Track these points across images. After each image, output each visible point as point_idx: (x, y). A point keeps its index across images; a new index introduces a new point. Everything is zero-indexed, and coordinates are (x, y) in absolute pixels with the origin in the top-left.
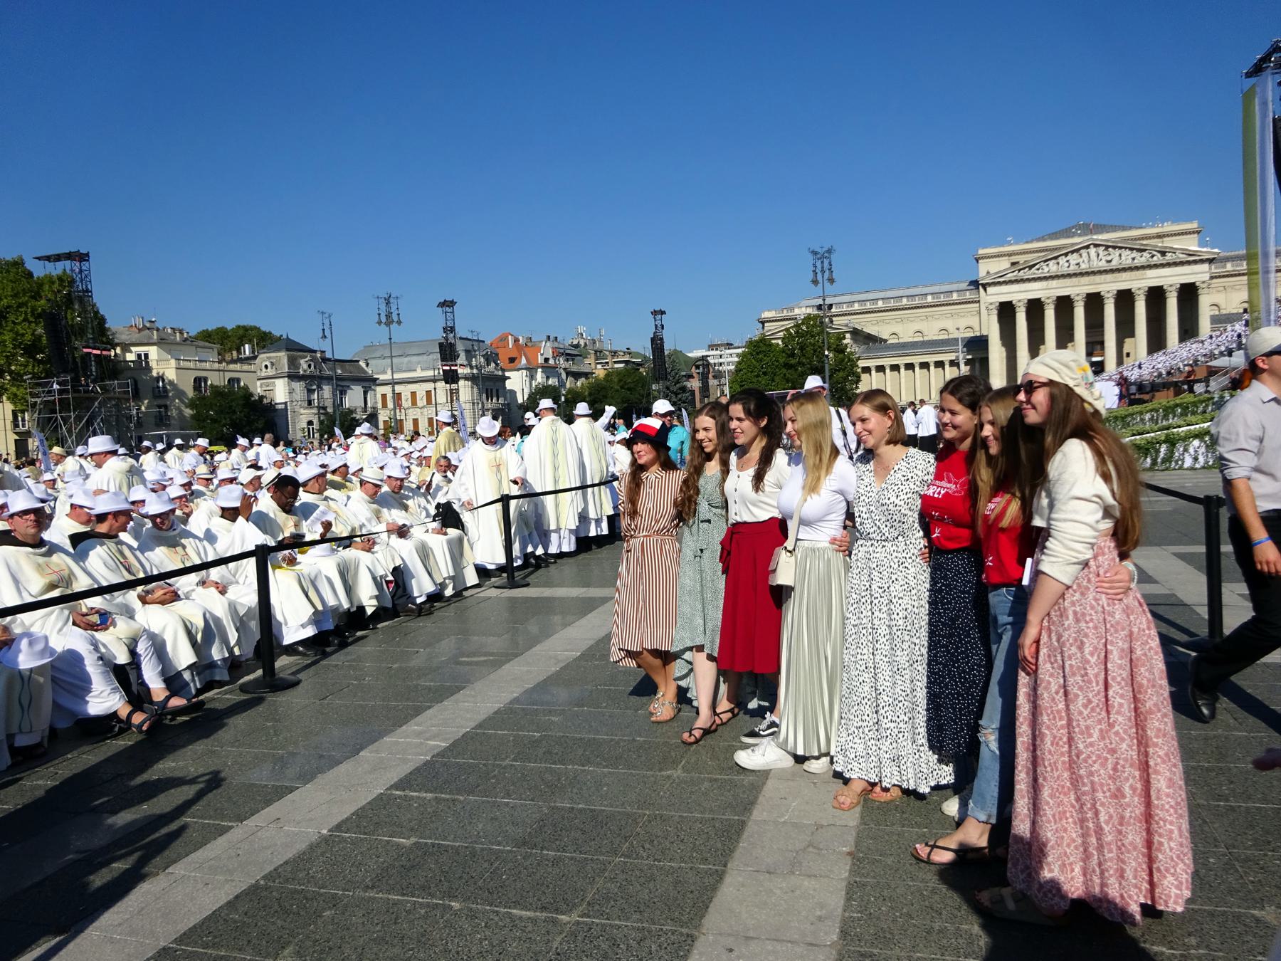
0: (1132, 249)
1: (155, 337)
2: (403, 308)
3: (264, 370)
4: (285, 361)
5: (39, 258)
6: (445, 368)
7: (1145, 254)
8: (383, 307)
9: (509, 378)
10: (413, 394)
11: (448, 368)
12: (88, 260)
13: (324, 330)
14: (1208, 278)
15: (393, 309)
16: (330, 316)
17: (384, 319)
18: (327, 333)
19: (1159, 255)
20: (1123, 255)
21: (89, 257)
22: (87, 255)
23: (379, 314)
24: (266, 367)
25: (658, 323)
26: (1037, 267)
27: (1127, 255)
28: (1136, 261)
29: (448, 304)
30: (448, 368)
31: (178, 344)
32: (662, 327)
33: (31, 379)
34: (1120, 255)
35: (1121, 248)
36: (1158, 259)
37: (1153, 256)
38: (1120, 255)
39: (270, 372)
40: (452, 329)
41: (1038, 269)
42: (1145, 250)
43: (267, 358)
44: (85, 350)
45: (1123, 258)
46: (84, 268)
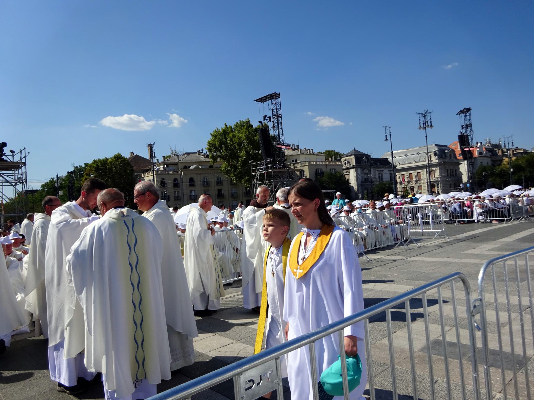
1: (300, 152)
2: (434, 118)
3: (344, 165)
4: (354, 160)
5: (256, 101)
6: (465, 149)
8: (422, 119)
9: (461, 164)
10: (411, 174)
11: (468, 149)
12: (280, 97)
13: (386, 136)
15: (429, 118)
16: (390, 128)
17: (422, 125)
18: (388, 137)
21: (280, 95)
22: (279, 94)
23: (420, 123)
24: (345, 164)
29: (466, 111)
30: (468, 149)
31: (309, 154)
33: (252, 162)
39: (348, 166)
40: (468, 126)
43: (346, 160)
44: (278, 146)
46: (277, 102)
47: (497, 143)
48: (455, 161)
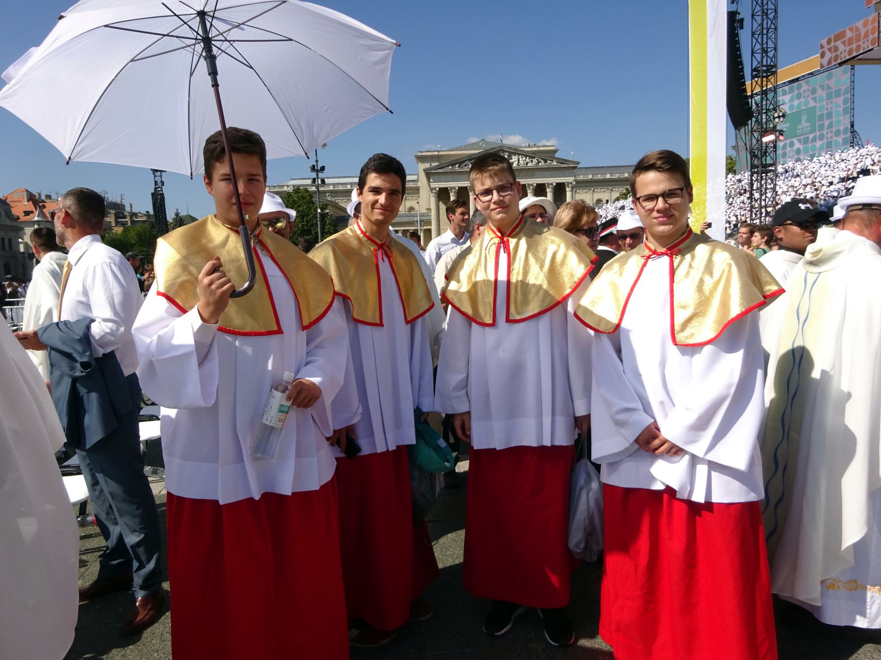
0: (526, 156)
7: (534, 160)
14: (572, 180)
19: (543, 162)
20: (520, 159)
25: (158, 179)
26: (465, 164)
27: (522, 160)
28: (528, 165)
32: (163, 183)
34: (519, 160)
35: (519, 154)
36: (542, 164)
37: (539, 162)
38: (519, 160)
41: (465, 166)
42: (534, 158)
45: (521, 162)
47: (119, 201)
48: (8, 222)
